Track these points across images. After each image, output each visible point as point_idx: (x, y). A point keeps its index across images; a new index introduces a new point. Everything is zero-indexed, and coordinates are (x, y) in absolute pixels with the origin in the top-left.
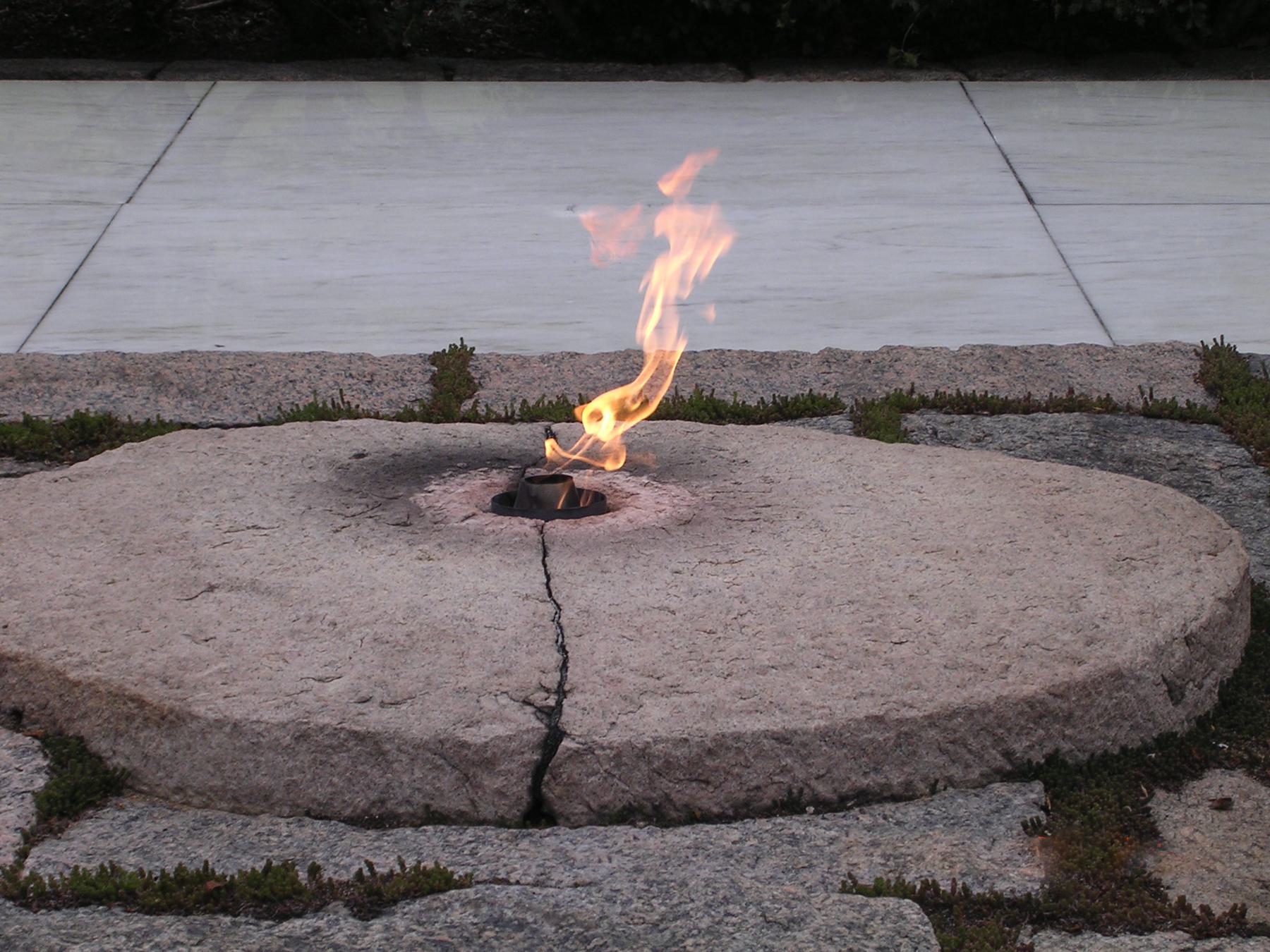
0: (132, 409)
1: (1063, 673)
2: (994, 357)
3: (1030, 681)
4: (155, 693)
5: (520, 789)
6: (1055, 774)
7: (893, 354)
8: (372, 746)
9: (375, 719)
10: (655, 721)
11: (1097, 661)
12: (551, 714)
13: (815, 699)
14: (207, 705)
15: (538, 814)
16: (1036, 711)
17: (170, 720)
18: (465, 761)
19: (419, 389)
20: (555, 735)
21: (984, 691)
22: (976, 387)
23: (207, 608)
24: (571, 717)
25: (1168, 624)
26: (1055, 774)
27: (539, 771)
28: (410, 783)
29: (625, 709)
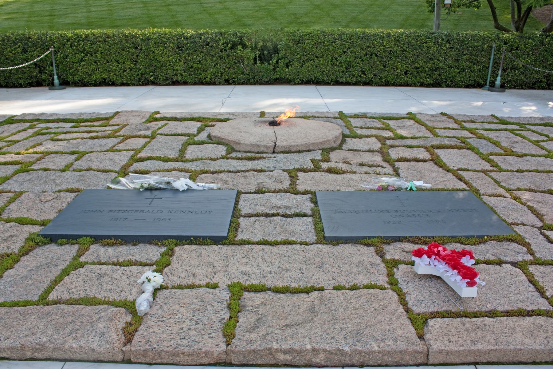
0: (231, 117)
1: (324, 140)
2: (318, 112)
3: (321, 140)
4: (237, 141)
5: (272, 150)
6: (323, 150)
7: (308, 112)
8: (258, 146)
9: (258, 143)
10: (285, 144)
11: (327, 139)
12: (275, 143)
13: (300, 142)
14: (242, 142)
15: (274, 152)
16: (321, 143)
17: (239, 144)
18: (267, 147)
19: (259, 115)
20: (276, 145)
21: (316, 141)
22: (317, 115)
23: (242, 134)
24: (277, 143)
25: (334, 136)
26: (323, 150)
27: (274, 148)
28: (262, 149)
29: (282, 143)
